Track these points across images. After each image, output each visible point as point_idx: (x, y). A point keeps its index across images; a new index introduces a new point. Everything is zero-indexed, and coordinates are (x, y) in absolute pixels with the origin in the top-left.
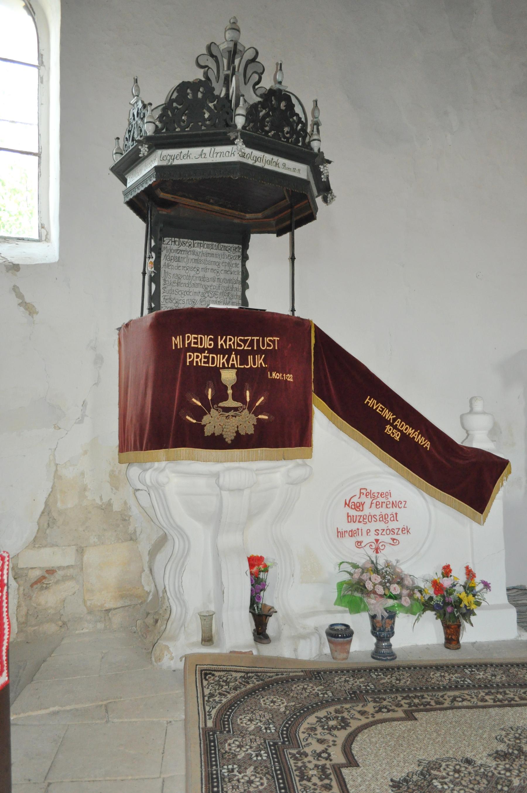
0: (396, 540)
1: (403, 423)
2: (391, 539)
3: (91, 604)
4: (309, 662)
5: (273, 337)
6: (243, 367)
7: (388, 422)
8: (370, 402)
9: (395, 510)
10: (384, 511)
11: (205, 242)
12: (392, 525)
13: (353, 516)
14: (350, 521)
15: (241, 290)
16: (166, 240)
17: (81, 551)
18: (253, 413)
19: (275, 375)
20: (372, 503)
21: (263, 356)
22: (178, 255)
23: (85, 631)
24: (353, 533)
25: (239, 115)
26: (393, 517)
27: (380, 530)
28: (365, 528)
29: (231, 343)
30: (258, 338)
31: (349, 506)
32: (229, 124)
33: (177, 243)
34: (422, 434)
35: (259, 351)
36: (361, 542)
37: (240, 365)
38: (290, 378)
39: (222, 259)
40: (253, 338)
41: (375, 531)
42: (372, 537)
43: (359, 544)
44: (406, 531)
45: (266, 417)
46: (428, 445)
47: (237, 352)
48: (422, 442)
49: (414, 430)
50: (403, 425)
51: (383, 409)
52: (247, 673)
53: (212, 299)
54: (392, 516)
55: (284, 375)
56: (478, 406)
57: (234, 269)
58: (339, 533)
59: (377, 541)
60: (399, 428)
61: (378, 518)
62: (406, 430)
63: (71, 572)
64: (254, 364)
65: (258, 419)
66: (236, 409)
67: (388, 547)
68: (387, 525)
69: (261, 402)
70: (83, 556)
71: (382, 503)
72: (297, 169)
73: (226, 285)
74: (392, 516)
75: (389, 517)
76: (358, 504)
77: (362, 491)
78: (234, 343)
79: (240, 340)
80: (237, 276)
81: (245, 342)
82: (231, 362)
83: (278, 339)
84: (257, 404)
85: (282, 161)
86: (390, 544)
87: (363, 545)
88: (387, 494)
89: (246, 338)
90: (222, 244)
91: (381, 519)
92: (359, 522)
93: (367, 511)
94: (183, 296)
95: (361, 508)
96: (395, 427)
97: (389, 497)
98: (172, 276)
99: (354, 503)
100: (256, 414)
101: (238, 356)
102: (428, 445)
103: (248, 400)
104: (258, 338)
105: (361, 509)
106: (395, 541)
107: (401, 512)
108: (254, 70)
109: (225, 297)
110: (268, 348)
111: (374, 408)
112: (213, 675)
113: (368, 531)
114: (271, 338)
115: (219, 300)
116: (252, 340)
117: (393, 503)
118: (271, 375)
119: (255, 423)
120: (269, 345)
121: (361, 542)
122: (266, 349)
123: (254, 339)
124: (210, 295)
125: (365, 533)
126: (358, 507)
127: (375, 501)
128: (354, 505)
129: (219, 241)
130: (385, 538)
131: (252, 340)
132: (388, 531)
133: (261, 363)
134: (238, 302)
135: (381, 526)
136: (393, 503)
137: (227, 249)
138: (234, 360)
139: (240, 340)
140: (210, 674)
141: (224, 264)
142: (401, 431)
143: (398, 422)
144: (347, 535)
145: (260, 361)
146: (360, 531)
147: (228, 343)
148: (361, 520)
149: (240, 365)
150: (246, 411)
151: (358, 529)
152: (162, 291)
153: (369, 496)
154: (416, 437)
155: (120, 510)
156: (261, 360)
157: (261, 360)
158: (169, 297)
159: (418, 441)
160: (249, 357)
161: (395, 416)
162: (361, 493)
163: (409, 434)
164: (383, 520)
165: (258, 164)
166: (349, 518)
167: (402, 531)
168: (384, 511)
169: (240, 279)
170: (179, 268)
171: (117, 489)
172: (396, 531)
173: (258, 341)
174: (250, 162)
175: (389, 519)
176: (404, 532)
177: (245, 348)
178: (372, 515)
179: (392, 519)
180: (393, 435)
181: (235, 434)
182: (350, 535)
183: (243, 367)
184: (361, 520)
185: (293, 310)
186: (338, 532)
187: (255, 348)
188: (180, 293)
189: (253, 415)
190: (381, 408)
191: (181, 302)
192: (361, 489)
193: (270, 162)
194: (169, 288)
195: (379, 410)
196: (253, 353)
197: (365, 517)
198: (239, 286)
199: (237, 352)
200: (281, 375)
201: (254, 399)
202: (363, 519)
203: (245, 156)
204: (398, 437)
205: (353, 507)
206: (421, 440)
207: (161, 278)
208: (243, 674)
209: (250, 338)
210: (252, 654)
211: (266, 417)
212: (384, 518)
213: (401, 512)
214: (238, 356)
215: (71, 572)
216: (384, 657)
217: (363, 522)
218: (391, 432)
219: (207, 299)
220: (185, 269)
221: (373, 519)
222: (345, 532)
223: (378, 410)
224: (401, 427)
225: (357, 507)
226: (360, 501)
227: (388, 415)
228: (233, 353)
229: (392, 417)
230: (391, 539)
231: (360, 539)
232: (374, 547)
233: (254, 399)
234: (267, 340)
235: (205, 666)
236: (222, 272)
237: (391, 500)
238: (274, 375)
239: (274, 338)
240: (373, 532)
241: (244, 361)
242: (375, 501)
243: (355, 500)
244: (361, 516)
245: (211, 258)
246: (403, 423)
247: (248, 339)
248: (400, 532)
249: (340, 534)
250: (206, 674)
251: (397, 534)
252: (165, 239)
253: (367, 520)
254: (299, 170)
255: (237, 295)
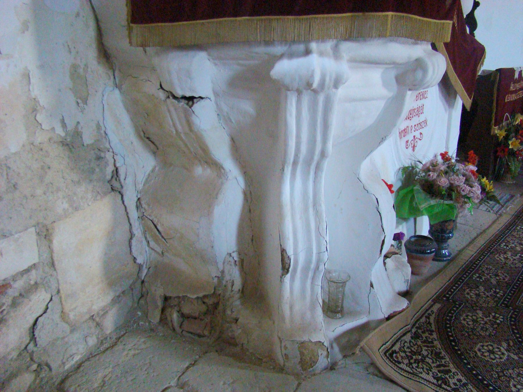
3: (75, 315)
17: (45, 234)
23: (77, 358)
63: (34, 276)
70: (51, 241)
155: (93, 141)
171: (85, 102)
215: (34, 276)
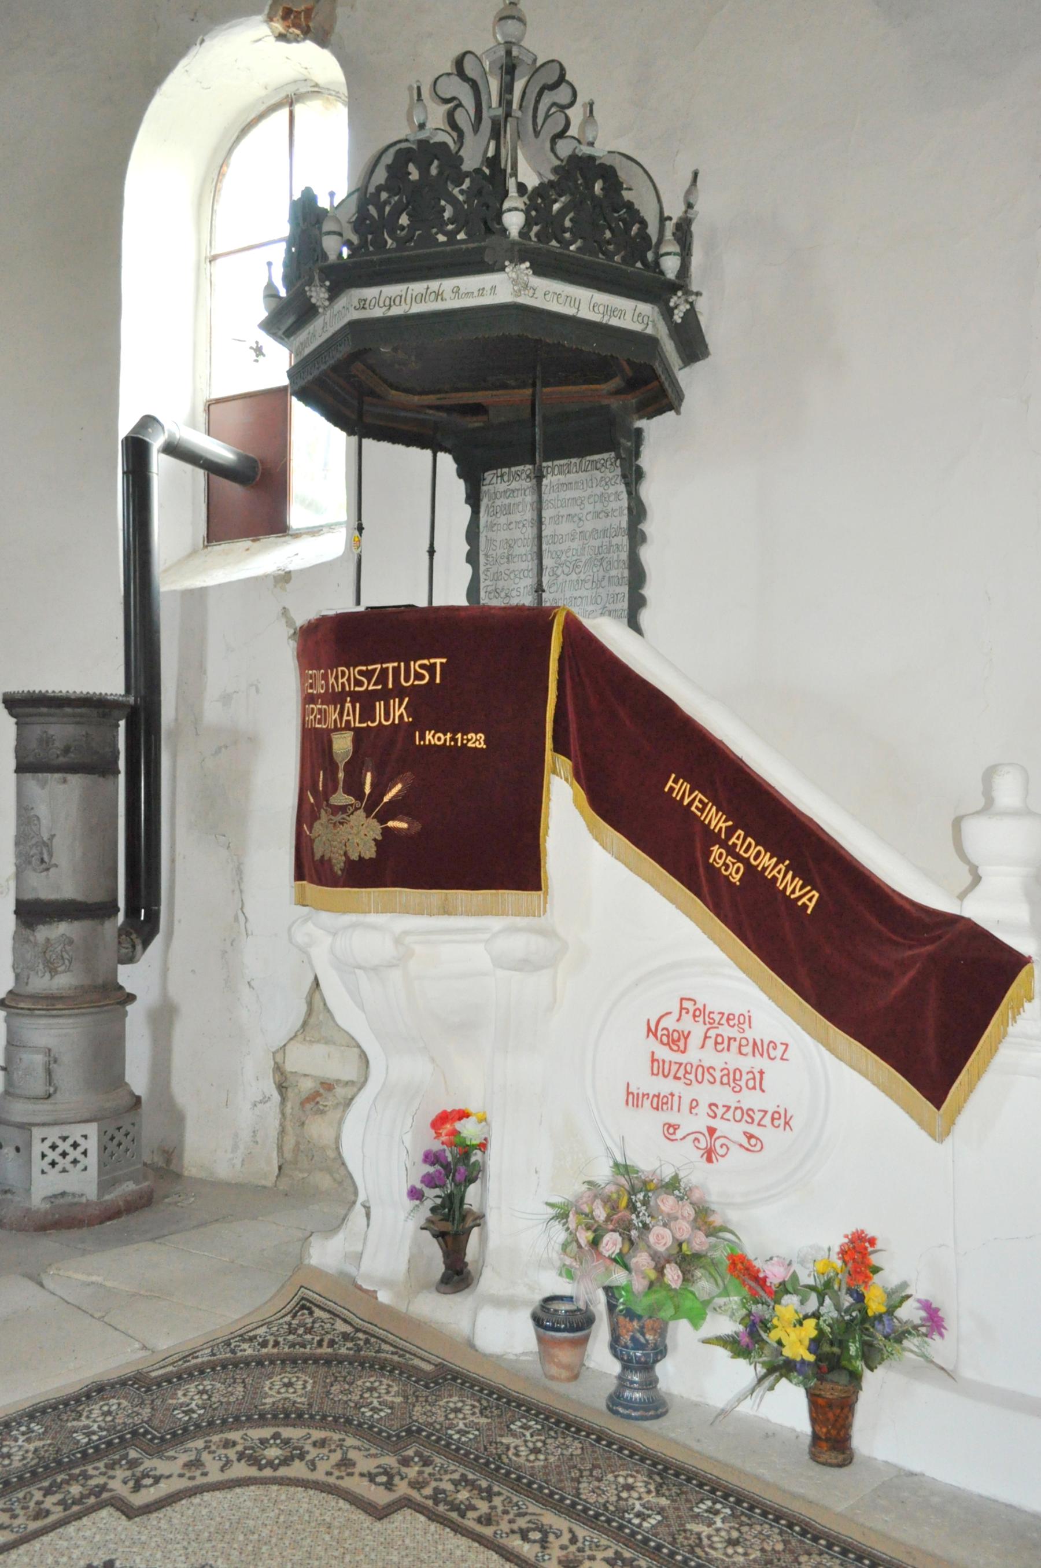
0: (757, 1139)
1: (749, 839)
2: (745, 1133)
4: (495, 1360)
5: (428, 658)
6: (365, 725)
7: (711, 837)
8: (677, 787)
9: (759, 1063)
10: (732, 1060)
11: (557, 462)
12: (751, 1099)
13: (664, 1062)
14: (655, 1072)
15: (626, 548)
16: (488, 475)
18: (374, 817)
19: (431, 738)
20: (706, 1037)
21: (407, 699)
22: (507, 501)
24: (660, 1103)
25: (329, 233)
26: (754, 1079)
27: (720, 1106)
28: (689, 1094)
29: (345, 680)
30: (396, 664)
31: (655, 1035)
32: (490, 222)
33: (506, 478)
34: (798, 870)
35: (400, 692)
36: (676, 1127)
37: (360, 722)
38: (477, 741)
39: (589, 490)
40: (384, 666)
41: (710, 1105)
42: (700, 1122)
43: (671, 1128)
44: (782, 1121)
45: (405, 825)
46: (810, 899)
47: (355, 697)
48: (793, 892)
49: (775, 860)
50: (750, 845)
51: (705, 805)
52: (358, 1330)
53: (568, 578)
54: (751, 1076)
55: (459, 736)
56: (1008, 791)
57: (614, 505)
58: (631, 1097)
59: (712, 1131)
60: (741, 852)
61: (718, 1075)
62: (756, 858)
64: (387, 719)
65: (387, 832)
66: (343, 809)
67: (734, 1149)
68: (738, 1096)
69: (396, 795)
71: (730, 1039)
72: (488, 288)
73: (597, 543)
74: (751, 1076)
75: (745, 1077)
76: (676, 1035)
77: (686, 1004)
78: (349, 680)
79: (361, 673)
80: (619, 518)
81: (368, 675)
82: (345, 718)
83: (444, 660)
84: (386, 799)
85: (447, 284)
86: (741, 1145)
87: (680, 1134)
88: (742, 1018)
89: (370, 668)
90: (588, 458)
91: (725, 1080)
92: (676, 1078)
93: (693, 1055)
94: (517, 580)
95: (681, 1044)
96: (731, 851)
97: (746, 1026)
98: (498, 544)
99: (667, 1029)
100: (382, 819)
101: (358, 705)
102: (810, 900)
103: (368, 790)
104: (396, 664)
105: (682, 1048)
106: (753, 1141)
107: (774, 1071)
108: (540, 85)
109: (595, 569)
110: (416, 683)
111: (686, 802)
112: (311, 1313)
113: (694, 1103)
114: (426, 662)
115: (582, 576)
116: (384, 672)
117: (755, 1043)
118: (422, 737)
119: (379, 838)
120: (420, 677)
121: (676, 1127)
122: (412, 684)
123: (387, 668)
124: (566, 570)
125: (685, 1107)
126: (676, 1041)
127: (712, 1033)
128: (668, 1036)
129: (581, 454)
130: (731, 1130)
131: (384, 672)
132: (738, 1113)
133: (401, 716)
134: (622, 574)
135: (724, 1095)
136: (755, 1043)
137: (599, 465)
138: (352, 714)
139: (361, 673)
140: (309, 1309)
141: (591, 500)
142: (746, 862)
143: (738, 838)
144: (647, 1103)
145: (399, 711)
146: (676, 1098)
147: (340, 681)
148: (680, 1074)
149: (360, 722)
150: (361, 813)
151: (672, 1095)
152: (482, 577)
153: (701, 1019)
154: (780, 877)
156: (402, 709)
157: (402, 709)
158: (493, 588)
159: (785, 888)
160: (377, 704)
161: (730, 823)
162: (682, 1008)
163: (764, 869)
164: (728, 1084)
165: (396, 311)
166: (656, 1064)
167: (773, 1119)
168: (732, 1060)
169: (624, 524)
170: (511, 526)
172: (757, 1116)
173: (397, 671)
174: (378, 313)
175: (743, 1083)
176: (776, 1123)
177: (371, 688)
178: (706, 1064)
179: (751, 1084)
180: (726, 870)
181: (344, 858)
182: (655, 1105)
183: (365, 725)
184: (680, 1074)
185: (539, 589)
186: (628, 1093)
187: (390, 686)
188: (512, 576)
189: (374, 823)
190: (701, 801)
191: (514, 593)
192: (682, 999)
193: (422, 298)
194: (494, 569)
195: (697, 808)
196: (385, 695)
197: (689, 1068)
198: (624, 541)
199: (355, 697)
200: (449, 735)
201: (380, 788)
202: (685, 1073)
203: (367, 306)
204: (738, 877)
205: (665, 1039)
206: (790, 885)
207: (481, 553)
208: (348, 1329)
209: (379, 666)
210: (376, 1298)
211: (405, 825)
212: (731, 1078)
213: (774, 1071)
214: (358, 705)
216: (626, 1407)
217: (683, 1080)
218: (721, 862)
219: (560, 580)
220: (521, 525)
221: (707, 1076)
222: (644, 1095)
223: (693, 809)
224: (746, 851)
225: (673, 1041)
226: (679, 1027)
227: (716, 820)
228: (349, 699)
229: (724, 825)
230: (745, 1133)
231: (673, 1118)
232: (703, 1144)
233: (380, 788)
234: (415, 666)
235: (311, 1293)
236: (589, 517)
237: (750, 1034)
238: (429, 736)
239: (432, 661)
240: (703, 1109)
241: (367, 713)
242: (712, 1033)
243: (669, 1023)
244: (681, 1064)
245: (568, 492)
246: (749, 839)
247: (376, 669)
248: (767, 1120)
249: (634, 1098)
250: (303, 1307)
251: (759, 1124)
252: (486, 474)
253: (692, 1077)
254: (494, 288)
255: (618, 561)
